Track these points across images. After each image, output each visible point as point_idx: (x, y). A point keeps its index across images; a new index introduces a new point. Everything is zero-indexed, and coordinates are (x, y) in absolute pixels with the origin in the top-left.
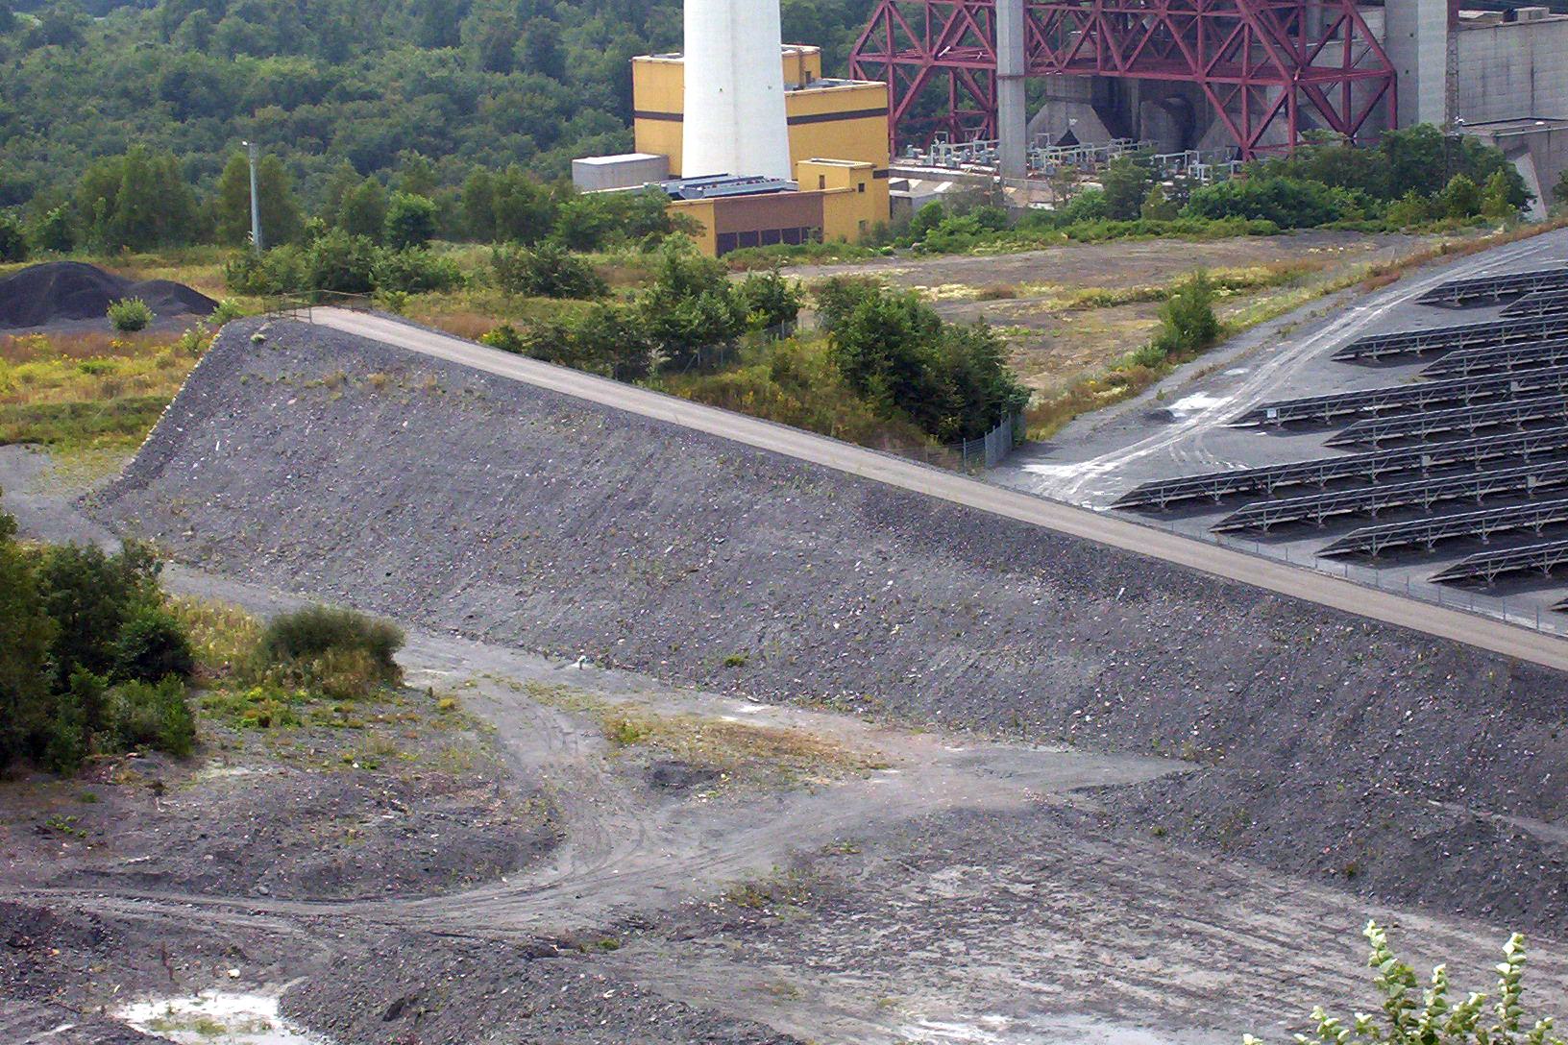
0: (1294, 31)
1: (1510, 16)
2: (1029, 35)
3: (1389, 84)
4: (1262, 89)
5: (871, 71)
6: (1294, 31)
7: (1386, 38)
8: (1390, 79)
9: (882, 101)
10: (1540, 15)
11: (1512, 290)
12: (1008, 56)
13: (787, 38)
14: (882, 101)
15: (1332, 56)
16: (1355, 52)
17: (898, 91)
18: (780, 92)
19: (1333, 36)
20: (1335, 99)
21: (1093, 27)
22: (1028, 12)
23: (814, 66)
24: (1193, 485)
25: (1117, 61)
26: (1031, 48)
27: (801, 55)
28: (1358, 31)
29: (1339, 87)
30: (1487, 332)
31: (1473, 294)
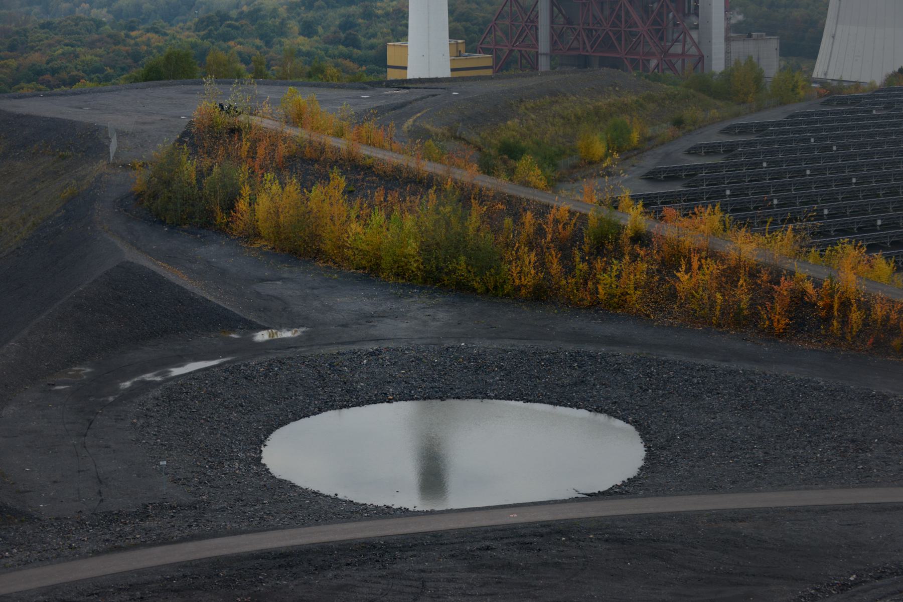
0: (662, 39)
1: (750, 36)
2: (552, 36)
3: (701, 59)
4: (648, 61)
5: (485, 51)
6: (662, 39)
7: (699, 42)
8: (701, 58)
9: (489, 62)
10: (762, 36)
11: (761, 128)
12: (544, 45)
13: (450, 37)
14: (489, 62)
15: (677, 49)
16: (687, 47)
17: (497, 59)
18: (448, 57)
19: (677, 41)
20: (678, 65)
21: (578, 35)
22: (552, 27)
23: (462, 48)
24: (674, 170)
25: (589, 48)
26: (553, 43)
27: (457, 43)
28: (688, 39)
29: (680, 61)
30: (714, 168)
31: (744, 129)
